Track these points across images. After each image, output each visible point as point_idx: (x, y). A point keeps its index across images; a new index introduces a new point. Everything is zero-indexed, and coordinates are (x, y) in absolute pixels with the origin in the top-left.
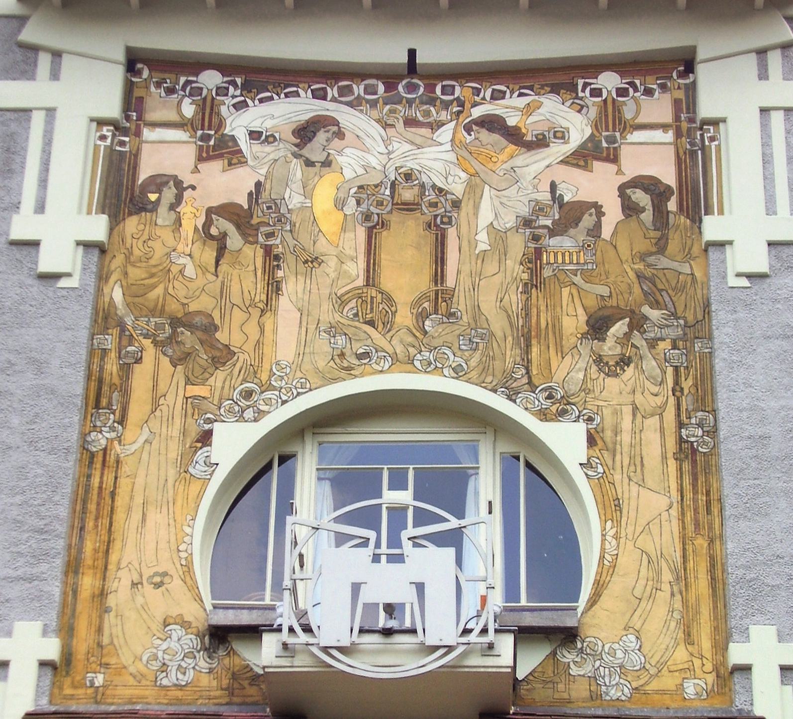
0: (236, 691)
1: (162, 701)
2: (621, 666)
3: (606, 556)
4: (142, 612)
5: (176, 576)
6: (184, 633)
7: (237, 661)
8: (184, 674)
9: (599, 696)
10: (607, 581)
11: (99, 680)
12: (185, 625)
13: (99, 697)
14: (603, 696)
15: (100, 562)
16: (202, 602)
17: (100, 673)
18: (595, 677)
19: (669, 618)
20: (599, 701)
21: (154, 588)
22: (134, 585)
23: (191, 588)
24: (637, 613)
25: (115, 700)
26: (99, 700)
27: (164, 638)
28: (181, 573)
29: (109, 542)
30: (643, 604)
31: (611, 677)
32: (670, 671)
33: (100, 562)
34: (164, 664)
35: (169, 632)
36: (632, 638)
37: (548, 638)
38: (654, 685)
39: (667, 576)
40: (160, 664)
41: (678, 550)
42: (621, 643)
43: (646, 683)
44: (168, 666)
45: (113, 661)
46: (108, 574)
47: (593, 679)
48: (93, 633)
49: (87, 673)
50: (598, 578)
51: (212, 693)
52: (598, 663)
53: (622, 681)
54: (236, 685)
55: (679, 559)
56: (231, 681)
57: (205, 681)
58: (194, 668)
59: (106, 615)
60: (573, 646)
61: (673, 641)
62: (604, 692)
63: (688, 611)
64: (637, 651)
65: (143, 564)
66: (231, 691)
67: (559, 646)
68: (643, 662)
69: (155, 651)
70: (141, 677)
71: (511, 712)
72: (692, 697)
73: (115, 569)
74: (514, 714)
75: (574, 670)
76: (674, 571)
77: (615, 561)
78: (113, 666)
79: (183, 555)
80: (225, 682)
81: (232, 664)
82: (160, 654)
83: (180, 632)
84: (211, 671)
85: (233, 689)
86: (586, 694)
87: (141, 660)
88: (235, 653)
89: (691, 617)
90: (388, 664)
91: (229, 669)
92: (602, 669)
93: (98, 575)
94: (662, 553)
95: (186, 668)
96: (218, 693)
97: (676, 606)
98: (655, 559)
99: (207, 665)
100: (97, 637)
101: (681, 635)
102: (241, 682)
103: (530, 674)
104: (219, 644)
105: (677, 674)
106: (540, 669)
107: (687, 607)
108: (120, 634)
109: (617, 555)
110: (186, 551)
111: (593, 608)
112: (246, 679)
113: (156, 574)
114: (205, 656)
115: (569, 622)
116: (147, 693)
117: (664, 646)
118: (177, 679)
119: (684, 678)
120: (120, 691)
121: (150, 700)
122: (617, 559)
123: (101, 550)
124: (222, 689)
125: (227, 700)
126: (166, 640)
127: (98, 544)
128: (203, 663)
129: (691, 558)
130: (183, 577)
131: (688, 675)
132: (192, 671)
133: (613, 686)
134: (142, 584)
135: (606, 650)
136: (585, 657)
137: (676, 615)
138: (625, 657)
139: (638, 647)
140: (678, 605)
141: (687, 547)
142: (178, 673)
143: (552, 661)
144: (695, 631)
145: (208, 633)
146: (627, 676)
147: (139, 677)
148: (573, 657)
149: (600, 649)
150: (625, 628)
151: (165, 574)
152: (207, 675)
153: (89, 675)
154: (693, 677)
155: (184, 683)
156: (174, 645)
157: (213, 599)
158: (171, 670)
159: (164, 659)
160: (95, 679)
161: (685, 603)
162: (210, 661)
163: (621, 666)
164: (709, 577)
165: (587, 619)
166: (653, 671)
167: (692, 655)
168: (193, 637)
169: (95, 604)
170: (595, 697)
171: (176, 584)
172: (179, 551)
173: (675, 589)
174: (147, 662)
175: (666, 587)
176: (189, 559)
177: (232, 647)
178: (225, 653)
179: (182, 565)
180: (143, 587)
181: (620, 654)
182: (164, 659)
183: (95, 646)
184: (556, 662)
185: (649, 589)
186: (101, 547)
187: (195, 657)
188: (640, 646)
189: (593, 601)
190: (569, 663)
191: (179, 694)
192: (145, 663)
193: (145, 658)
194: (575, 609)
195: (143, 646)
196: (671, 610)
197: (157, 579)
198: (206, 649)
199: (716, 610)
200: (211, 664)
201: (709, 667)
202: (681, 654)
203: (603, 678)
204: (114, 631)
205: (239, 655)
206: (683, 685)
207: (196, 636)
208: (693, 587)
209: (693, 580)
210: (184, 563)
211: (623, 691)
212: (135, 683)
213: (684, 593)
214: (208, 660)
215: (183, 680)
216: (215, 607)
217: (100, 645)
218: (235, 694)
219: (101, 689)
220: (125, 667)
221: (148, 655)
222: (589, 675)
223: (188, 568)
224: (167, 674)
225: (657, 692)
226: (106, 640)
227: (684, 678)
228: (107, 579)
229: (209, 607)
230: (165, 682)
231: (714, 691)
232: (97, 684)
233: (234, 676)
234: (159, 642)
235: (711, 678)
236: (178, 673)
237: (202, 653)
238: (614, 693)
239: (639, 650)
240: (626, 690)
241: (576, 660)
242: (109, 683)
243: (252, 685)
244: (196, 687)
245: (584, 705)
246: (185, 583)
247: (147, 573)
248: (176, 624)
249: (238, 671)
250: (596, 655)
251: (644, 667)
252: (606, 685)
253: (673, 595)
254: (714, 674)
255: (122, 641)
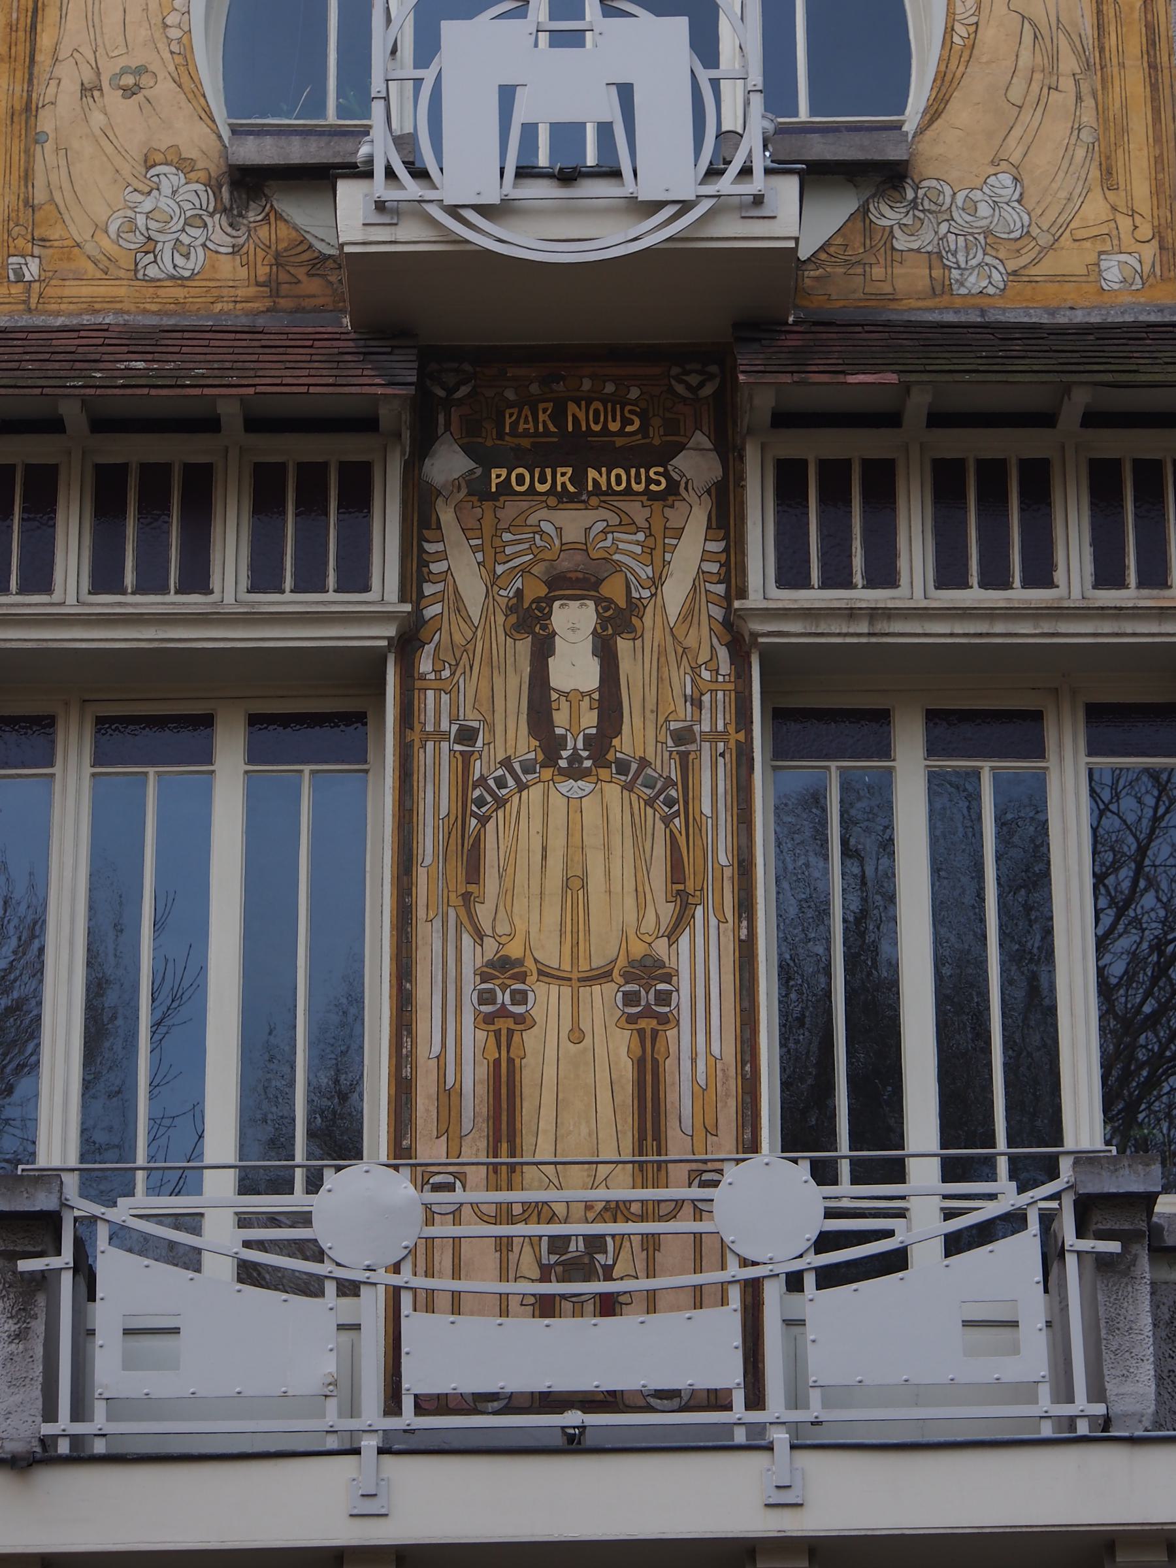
0: (284, 288)
1: (148, 306)
2: (988, 232)
3: (957, 27)
4: (104, 142)
5: (161, 75)
6: (183, 181)
7: (283, 231)
8: (187, 256)
9: (947, 289)
10: (958, 75)
11: (32, 269)
12: (184, 165)
13: (33, 301)
14: (955, 287)
15: (20, 47)
16: (214, 121)
17: (32, 256)
18: (940, 252)
19: (1073, 141)
20: (946, 297)
21: (123, 97)
22: (87, 90)
23: (191, 96)
24: (1017, 132)
25: (63, 307)
26: (33, 306)
27: (147, 189)
28: (172, 68)
29: (35, 11)
30: (1025, 117)
31: (968, 254)
32: (1075, 240)
33: (20, 47)
34: (149, 238)
35: (155, 179)
36: (1006, 179)
37: (851, 181)
38: (1047, 267)
39: (1069, 63)
40: (142, 239)
41: (1087, 13)
42: (985, 189)
43: (1035, 262)
44: (157, 242)
45: (55, 233)
46: (36, 70)
47: (936, 257)
48: (14, 183)
49: (9, 256)
50: (943, 68)
51: (240, 292)
52: (944, 228)
53: (988, 259)
54: (283, 277)
55: (1089, 32)
56: (274, 268)
57: (228, 268)
58: (204, 245)
59: (38, 147)
60: (898, 197)
61: (1081, 183)
62: (957, 281)
63: (1106, 129)
64: (1015, 204)
65: (100, 51)
66: (274, 285)
67: (873, 196)
68: (1026, 223)
69: (130, 213)
70: (107, 263)
71: (791, 319)
72: (1116, 287)
73: (49, 62)
74: (795, 323)
75: (902, 242)
76: (1080, 52)
77: (972, 36)
78: (56, 244)
79: (174, 33)
80: (263, 271)
81: (273, 237)
82: (141, 220)
83: (177, 177)
84: (236, 250)
85: (279, 284)
86: (923, 284)
87: (107, 232)
88: (279, 217)
89: (1112, 139)
90: (564, 238)
91: (270, 247)
92: (951, 237)
93: (19, 74)
94: (1058, 20)
95: (189, 245)
96: (252, 291)
97: (1084, 119)
98: (1045, 31)
99: (229, 239)
100: (23, 189)
101: (1095, 173)
102: (292, 270)
103: (822, 248)
104: (249, 199)
105: (1087, 244)
106: (839, 241)
107: (1106, 121)
108: (66, 185)
109: (977, 23)
110: (179, 26)
111: (935, 125)
112: (301, 264)
113: (125, 71)
114: (225, 224)
115: (894, 154)
116: (122, 292)
117: (1063, 194)
118: (175, 266)
119: (1101, 253)
120: (72, 289)
121: (126, 306)
122: (976, 32)
123: (21, 26)
124: (258, 284)
125: (268, 303)
126: (149, 193)
127: (15, 16)
128: (219, 234)
129: (1112, 28)
130: (175, 75)
131: (1108, 248)
132: (200, 250)
133: (973, 268)
134: (101, 90)
135: (960, 204)
136: (921, 215)
137: (1086, 135)
138: (993, 216)
139: (1016, 196)
140: (1088, 117)
141: (1105, 8)
142: (176, 255)
143: (861, 224)
144: (1120, 163)
145: (225, 180)
146: (997, 250)
147: (106, 267)
148: (898, 216)
149: (948, 200)
150: (992, 161)
151: (141, 70)
152: (230, 257)
153: (12, 260)
154: (1116, 249)
155: (187, 274)
156: (166, 204)
157: (229, 117)
158: (161, 250)
159: (148, 229)
160: (24, 267)
161: (1101, 111)
162: (234, 233)
163: (988, 232)
164: (1145, 65)
165: (926, 147)
166: (1045, 240)
167: (1114, 208)
168: (200, 187)
169: (16, 127)
170: (939, 289)
171: (163, 89)
172: (166, 26)
173: (1085, 88)
174: (119, 236)
175: (1067, 84)
176: (185, 40)
177: (272, 206)
178: (260, 218)
179: (172, 53)
180: (102, 95)
181: (984, 210)
182: (148, 229)
183: (21, 203)
184: (869, 228)
185: (1035, 87)
186: (22, 20)
187: (206, 226)
188: (1021, 194)
189: (934, 112)
190: (892, 227)
191: (179, 293)
192: (113, 236)
193: (113, 229)
194: (898, 126)
195: (109, 205)
196: (1076, 126)
197: (129, 80)
198: (224, 210)
199: (1158, 126)
200: (234, 237)
201: (1145, 231)
202: (1095, 208)
203: (954, 254)
204: (54, 177)
205: (285, 220)
206: (1098, 265)
207: (205, 185)
208: (1117, 83)
209: (1116, 70)
210: (175, 47)
211: (990, 277)
212: (99, 275)
213: (1100, 93)
214: (229, 230)
215: (186, 267)
216: (235, 131)
217: (30, 205)
218: (282, 293)
219: (36, 286)
220: (78, 245)
221: (119, 221)
222: (929, 248)
223: (185, 56)
224: (155, 257)
225: (1053, 278)
226: (40, 196)
227: (1101, 253)
228: (35, 82)
229: (225, 133)
230: (153, 271)
231: (1154, 273)
232: (28, 277)
233: (279, 261)
234: (139, 198)
235: (1149, 252)
236: (176, 255)
237: (218, 216)
238: (974, 282)
239: (1019, 201)
240: (996, 276)
241: (904, 221)
242: (50, 274)
243: (313, 275)
244: (210, 280)
245: (920, 304)
246: (180, 86)
247: (109, 69)
248: (166, 164)
249: (286, 250)
250: (940, 212)
251: (1028, 232)
252: (959, 268)
253: (1079, 98)
254: (1155, 243)
255: (68, 195)
